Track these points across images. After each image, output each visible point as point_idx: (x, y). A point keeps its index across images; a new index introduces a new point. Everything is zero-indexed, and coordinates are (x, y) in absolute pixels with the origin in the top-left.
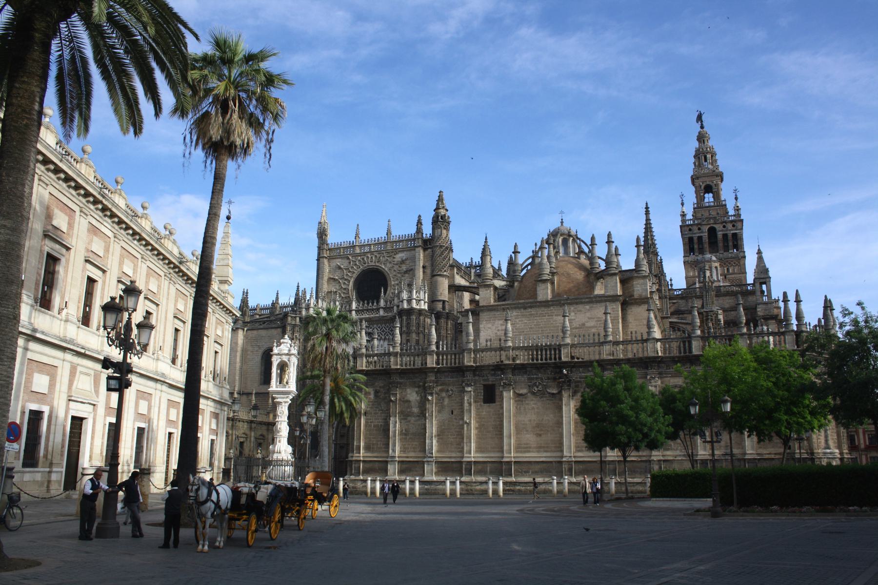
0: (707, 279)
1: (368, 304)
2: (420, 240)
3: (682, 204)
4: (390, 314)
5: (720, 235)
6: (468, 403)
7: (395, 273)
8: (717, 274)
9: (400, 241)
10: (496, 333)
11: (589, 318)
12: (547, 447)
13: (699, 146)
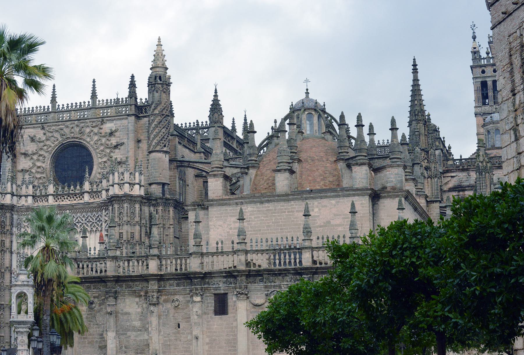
1: (69, 187)
2: (133, 106)
3: (474, 38)
4: (97, 200)
7: (102, 148)
9: (108, 107)
10: (228, 232)
11: (335, 215)
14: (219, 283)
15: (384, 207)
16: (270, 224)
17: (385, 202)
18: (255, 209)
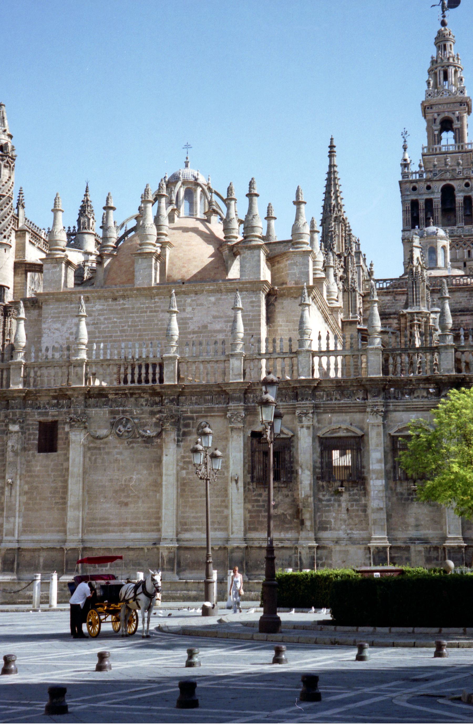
0: (415, 263)
3: (405, 148)
5: (459, 198)
6: (13, 451)
8: (445, 257)
10: (68, 339)
11: (214, 317)
12: (137, 524)
13: (438, 54)
14: (47, 406)
15: (283, 308)
16: (125, 328)
17: (284, 302)
18: (105, 308)
